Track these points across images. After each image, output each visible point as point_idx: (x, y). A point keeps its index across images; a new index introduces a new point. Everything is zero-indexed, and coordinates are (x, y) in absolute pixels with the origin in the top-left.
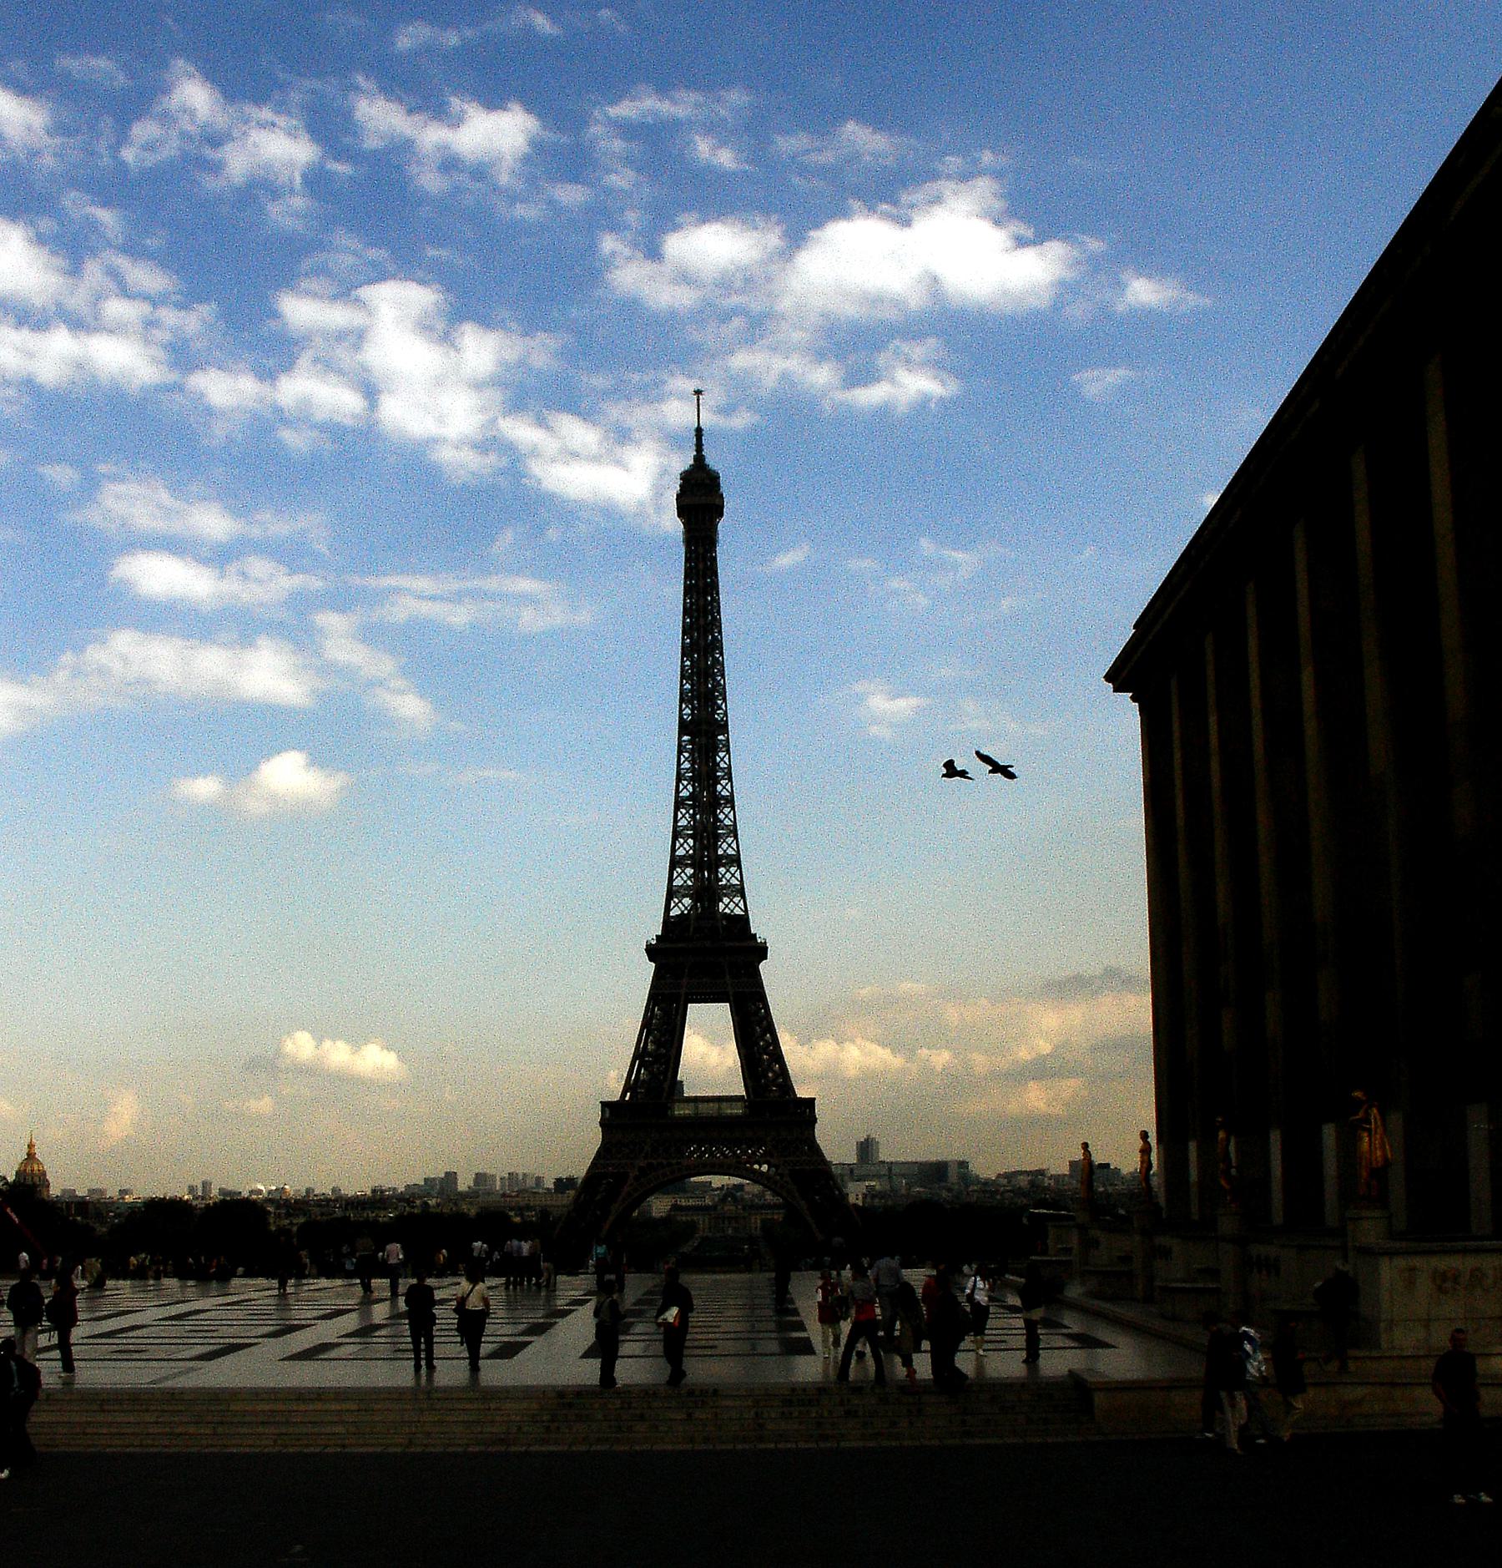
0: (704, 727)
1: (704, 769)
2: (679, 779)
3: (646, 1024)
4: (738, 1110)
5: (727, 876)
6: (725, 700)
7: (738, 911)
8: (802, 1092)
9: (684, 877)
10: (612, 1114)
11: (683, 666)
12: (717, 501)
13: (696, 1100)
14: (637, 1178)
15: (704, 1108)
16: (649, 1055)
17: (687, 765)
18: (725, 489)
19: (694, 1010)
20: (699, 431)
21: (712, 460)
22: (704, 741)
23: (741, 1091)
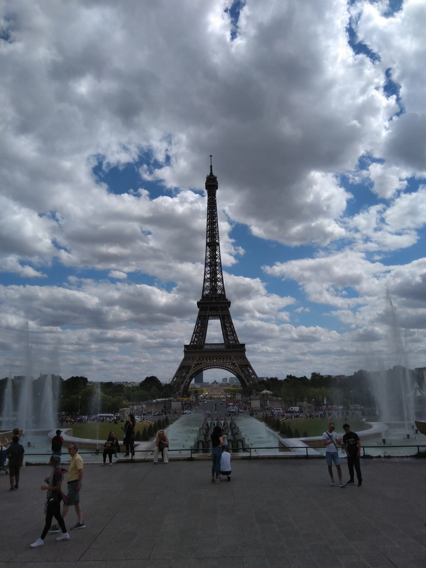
0: (213, 244)
1: (213, 255)
2: (206, 259)
4: (223, 347)
5: (219, 284)
6: (218, 237)
9: (207, 284)
11: (207, 228)
12: (216, 184)
14: (194, 367)
15: (213, 347)
17: (208, 253)
18: (218, 180)
20: (211, 166)
22: (213, 247)
23: (223, 342)
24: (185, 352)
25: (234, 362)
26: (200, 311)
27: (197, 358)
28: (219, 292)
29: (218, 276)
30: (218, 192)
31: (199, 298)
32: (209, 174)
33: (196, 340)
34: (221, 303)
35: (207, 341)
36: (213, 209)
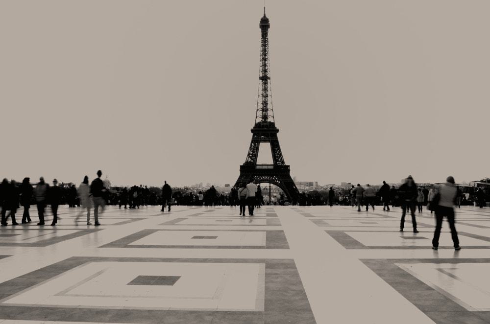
3: (251, 147)
4: (272, 167)
5: (270, 113)
7: (272, 121)
8: (287, 164)
9: (260, 113)
10: (243, 168)
13: (262, 165)
16: (251, 154)
19: (261, 144)
21: (267, 16)
23: (273, 163)
24: (241, 171)
25: (280, 180)
26: (253, 136)
27: (250, 176)
28: (269, 120)
29: (269, 106)
30: (270, 31)
31: (252, 126)
32: (262, 16)
33: (250, 160)
34: (271, 130)
35: (259, 161)
36: (266, 46)
